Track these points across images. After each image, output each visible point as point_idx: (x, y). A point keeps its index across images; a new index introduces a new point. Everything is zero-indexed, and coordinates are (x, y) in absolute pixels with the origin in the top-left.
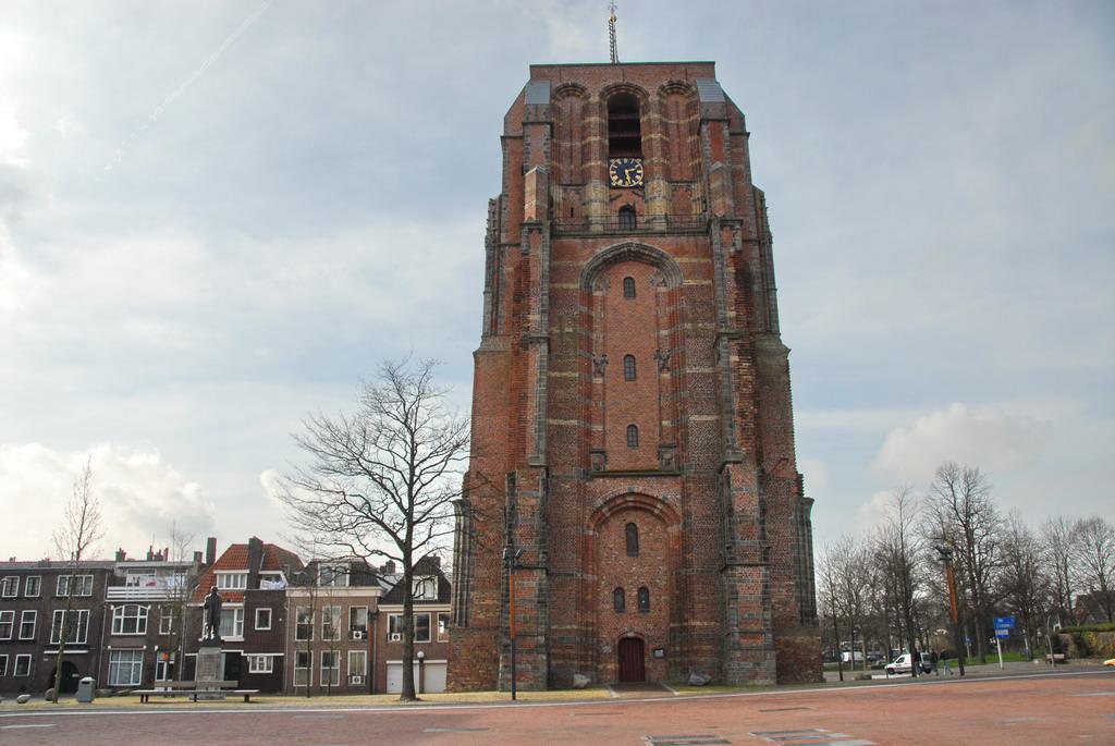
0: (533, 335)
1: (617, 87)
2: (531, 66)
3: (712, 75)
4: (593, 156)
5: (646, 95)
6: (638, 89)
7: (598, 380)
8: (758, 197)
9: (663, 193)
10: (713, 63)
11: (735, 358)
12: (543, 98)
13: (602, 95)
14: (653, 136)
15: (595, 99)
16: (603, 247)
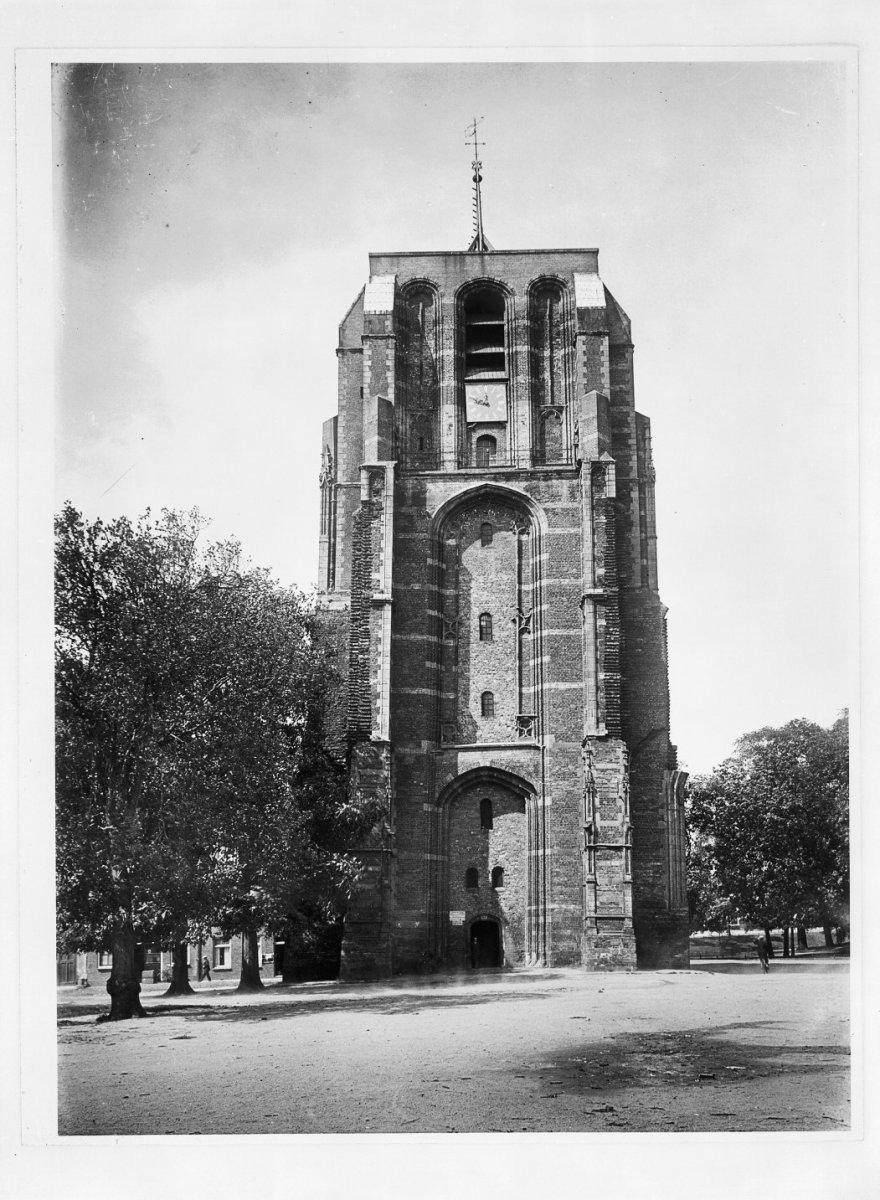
0: (377, 596)
1: (478, 282)
2: (371, 256)
3: (594, 269)
4: (447, 375)
5: (512, 293)
6: (502, 286)
7: (451, 643)
8: (643, 423)
9: (527, 422)
10: (595, 252)
11: (604, 623)
12: (381, 299)
13: (459, 295)
14: (519, 348)
15: (449, 300)
16: (459, 488)
